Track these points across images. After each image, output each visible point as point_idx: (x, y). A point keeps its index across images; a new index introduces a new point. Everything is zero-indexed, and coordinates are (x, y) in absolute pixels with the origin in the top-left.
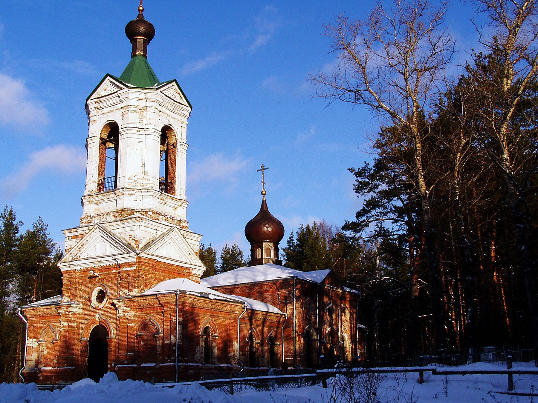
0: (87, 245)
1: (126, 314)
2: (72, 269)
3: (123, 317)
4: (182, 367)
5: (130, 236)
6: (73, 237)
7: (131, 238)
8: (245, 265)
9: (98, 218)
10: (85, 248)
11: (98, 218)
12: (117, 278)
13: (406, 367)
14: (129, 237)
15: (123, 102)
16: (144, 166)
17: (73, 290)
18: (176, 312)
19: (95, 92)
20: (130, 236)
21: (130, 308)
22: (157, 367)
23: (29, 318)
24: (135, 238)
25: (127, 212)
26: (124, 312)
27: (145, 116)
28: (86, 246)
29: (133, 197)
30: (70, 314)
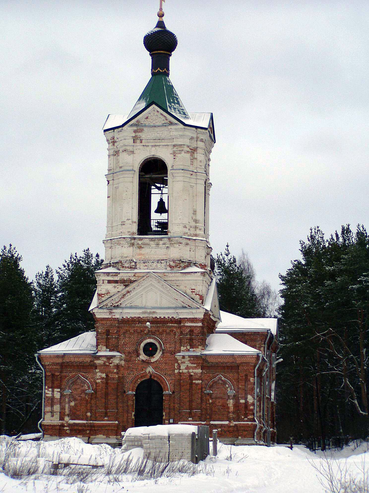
0: (133, 294)
1: (191, 371)
2: (113, 317)
3: (186, 373)
4: (130, 395)
5: (193, 291)
6: (109, 282)
7: (194, 292)
8: (273, 318)
9: (144, 265)
10: (129, 296)
11: (144, 265)
12: (175, 332)
13: (257, 377)
14: (191, 291)
15: (173, 138)
16: (195, 213)
17: (114, 339)
18: (254, 373)
19: (136, 117)
20: (193, 291)
21: (195, 365)
22: (231, 425)
23: (48, 365)
24: (199, 293)
25: (185, 263)
26: (187, 368)
27: (195, 157)
28: (132, 295)
29: (188, 248)
30: (111, 365)
